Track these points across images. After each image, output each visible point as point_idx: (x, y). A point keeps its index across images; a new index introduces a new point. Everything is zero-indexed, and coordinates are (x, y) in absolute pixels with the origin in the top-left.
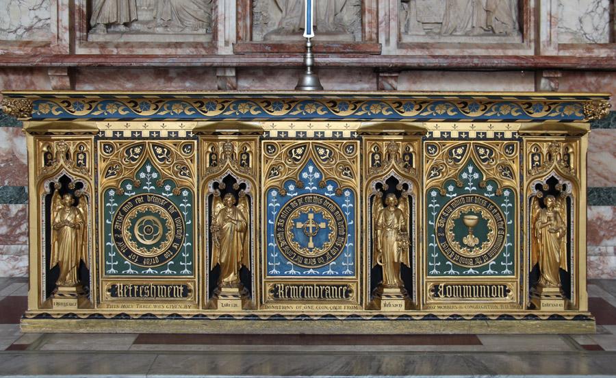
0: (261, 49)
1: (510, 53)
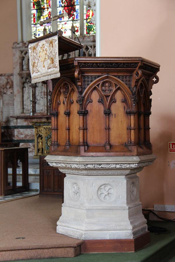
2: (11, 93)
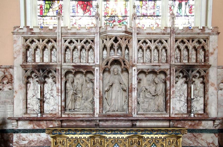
0: (105, 116)
1: (163, 116)
2: (10, 89)
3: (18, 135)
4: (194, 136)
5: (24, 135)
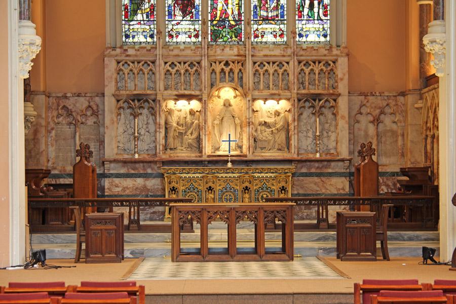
3: (110, 180)
4: (322, 181)
5: (117, 180)
